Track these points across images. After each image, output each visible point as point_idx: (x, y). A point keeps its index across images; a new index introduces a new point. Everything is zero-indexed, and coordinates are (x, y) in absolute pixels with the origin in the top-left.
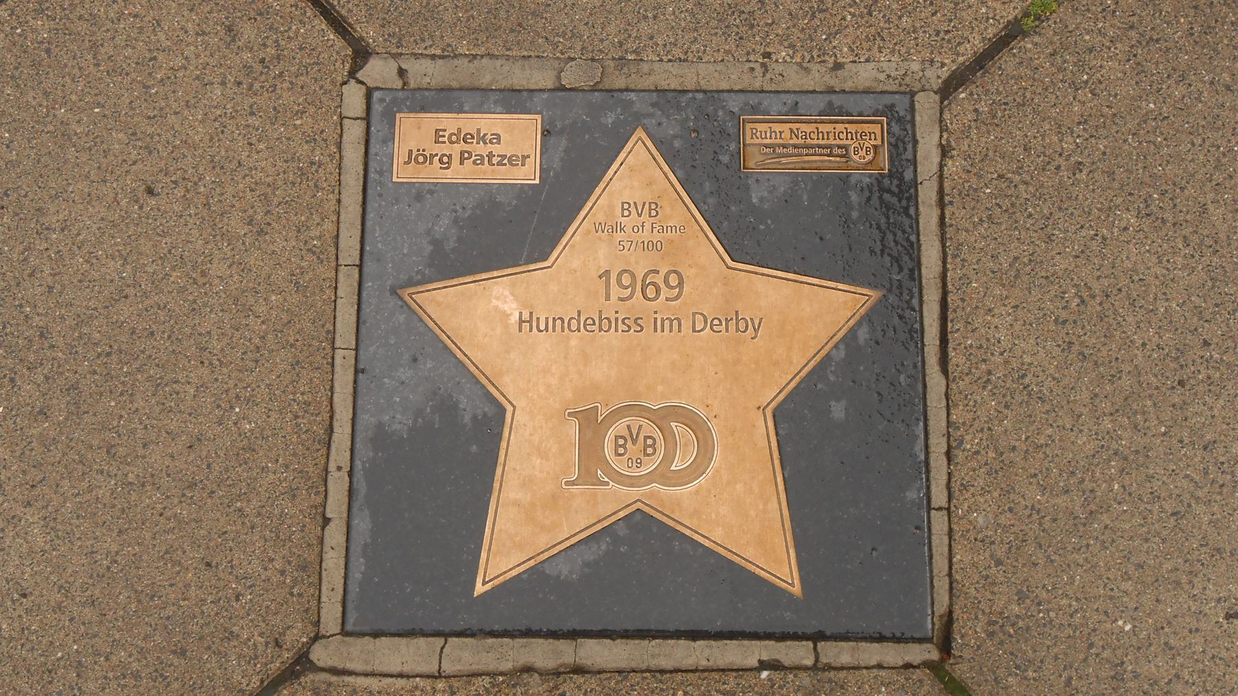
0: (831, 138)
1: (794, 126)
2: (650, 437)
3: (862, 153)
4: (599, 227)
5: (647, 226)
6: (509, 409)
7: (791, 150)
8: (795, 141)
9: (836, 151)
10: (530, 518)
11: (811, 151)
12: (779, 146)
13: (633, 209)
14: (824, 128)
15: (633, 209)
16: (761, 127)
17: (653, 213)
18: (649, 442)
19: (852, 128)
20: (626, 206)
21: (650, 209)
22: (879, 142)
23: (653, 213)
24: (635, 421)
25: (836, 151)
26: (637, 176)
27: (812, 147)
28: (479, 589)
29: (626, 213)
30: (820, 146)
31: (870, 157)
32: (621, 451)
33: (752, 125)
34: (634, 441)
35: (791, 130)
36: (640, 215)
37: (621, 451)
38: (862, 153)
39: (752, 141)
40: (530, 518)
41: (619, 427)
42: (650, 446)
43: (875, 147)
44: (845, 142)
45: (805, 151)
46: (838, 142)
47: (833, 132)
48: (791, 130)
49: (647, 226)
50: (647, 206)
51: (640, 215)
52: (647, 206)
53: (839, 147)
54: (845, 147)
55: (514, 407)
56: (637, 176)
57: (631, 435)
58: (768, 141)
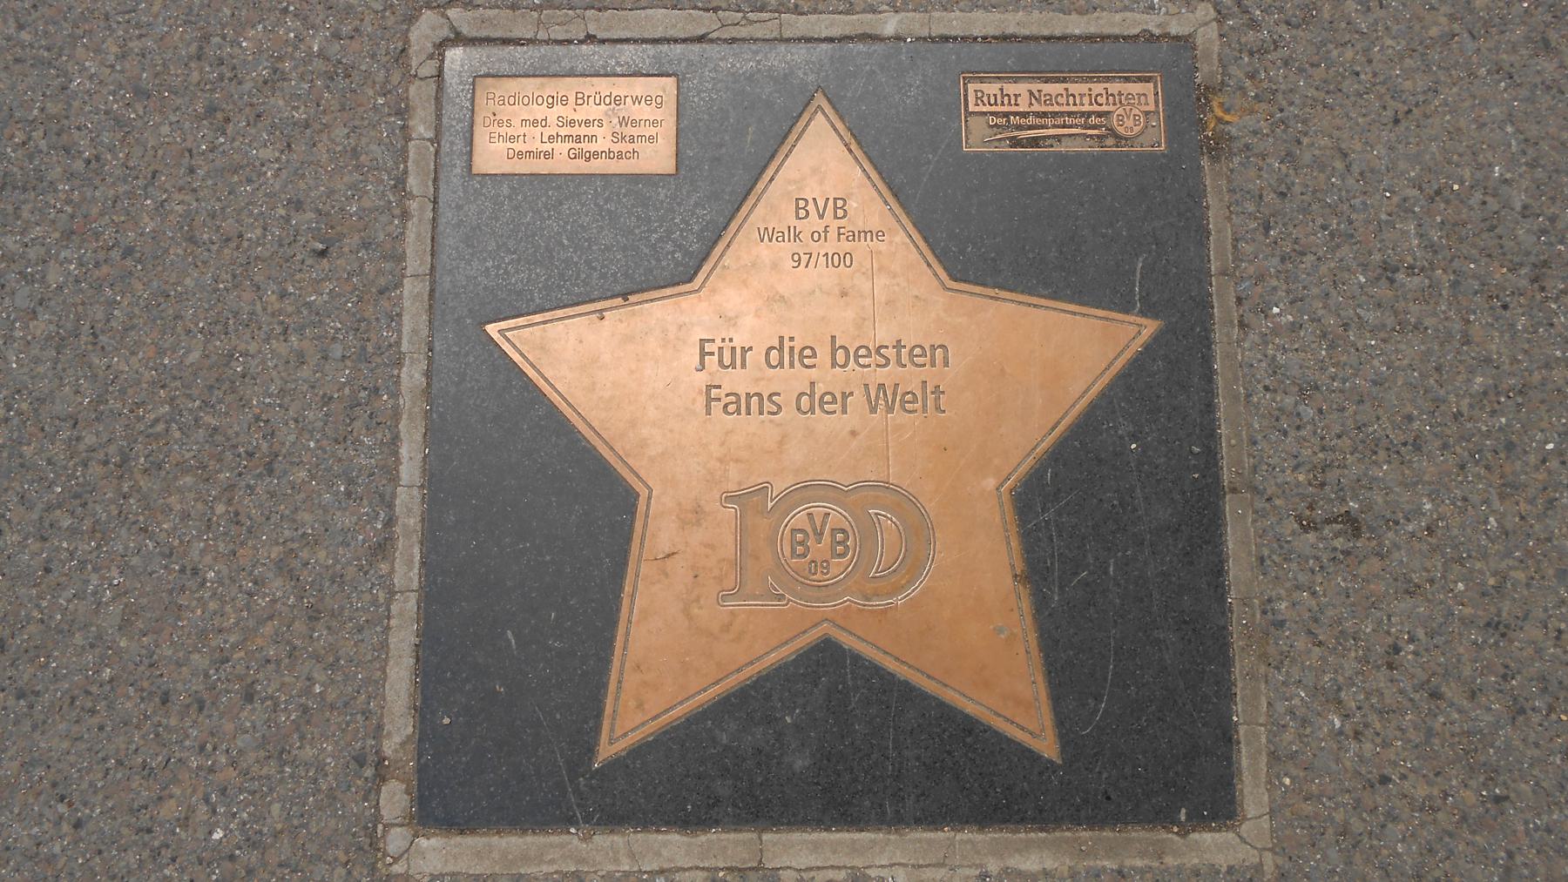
0: (1086, 100)
1: (1035, 87)
2: (843, 531)
3: (1129, 123)
4: (767, 235)
5: (833, 234)
6: (644, 493)
7: (1031, 120)
8: (1036, 108)
9: (1093, 120)
10: (674, 649)
11: (1060, 121)
12: (1016, 114)
13: (811, 207)
14: (1075, 88)
15: (811, 207)
16: (985, 87)
17: (840, 213)
18: (840, 536)
19: (1114, 88)
20: (802, 204)
21: (836, 208)
22: (1152, 108)
23: (840, 213)
24: (818, 509)
25: (1093, 120)
26: (821, 164)
27: (1062, 114)
28: (608, 749)
29: (802, 213)
30: (1070, 114)
31: (1137, 129)
32: (800, 549)
33: (979, 86)
34: (819, 535)
35: (1031, 93)
36: (821, 217)
37: (800, 549)
38: (1129, 123)
39: (977, 109)
40: (674, 649)
41: (798, 518)
42: (839, 543)
43: (1147, 113)
44: (1105, 108)
45: (1049, 122)
46: (1096, 108)
47: (1083, 94)
48: (1031, 93)
49: (833, 234)
50: (831, 202)
51: (821, 217)
52: (831, 202)
53: (1100, 115)
54: (1106, 114)
55: (651, 491)
56: (821, 164)
57: (814, 530)
58: (999, 109)
